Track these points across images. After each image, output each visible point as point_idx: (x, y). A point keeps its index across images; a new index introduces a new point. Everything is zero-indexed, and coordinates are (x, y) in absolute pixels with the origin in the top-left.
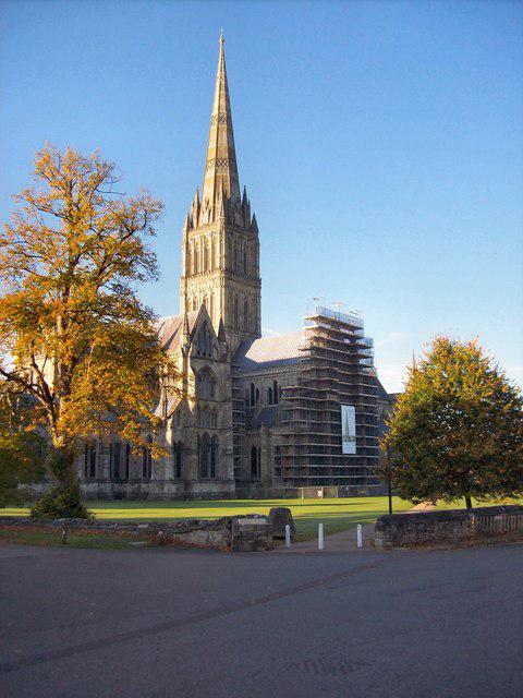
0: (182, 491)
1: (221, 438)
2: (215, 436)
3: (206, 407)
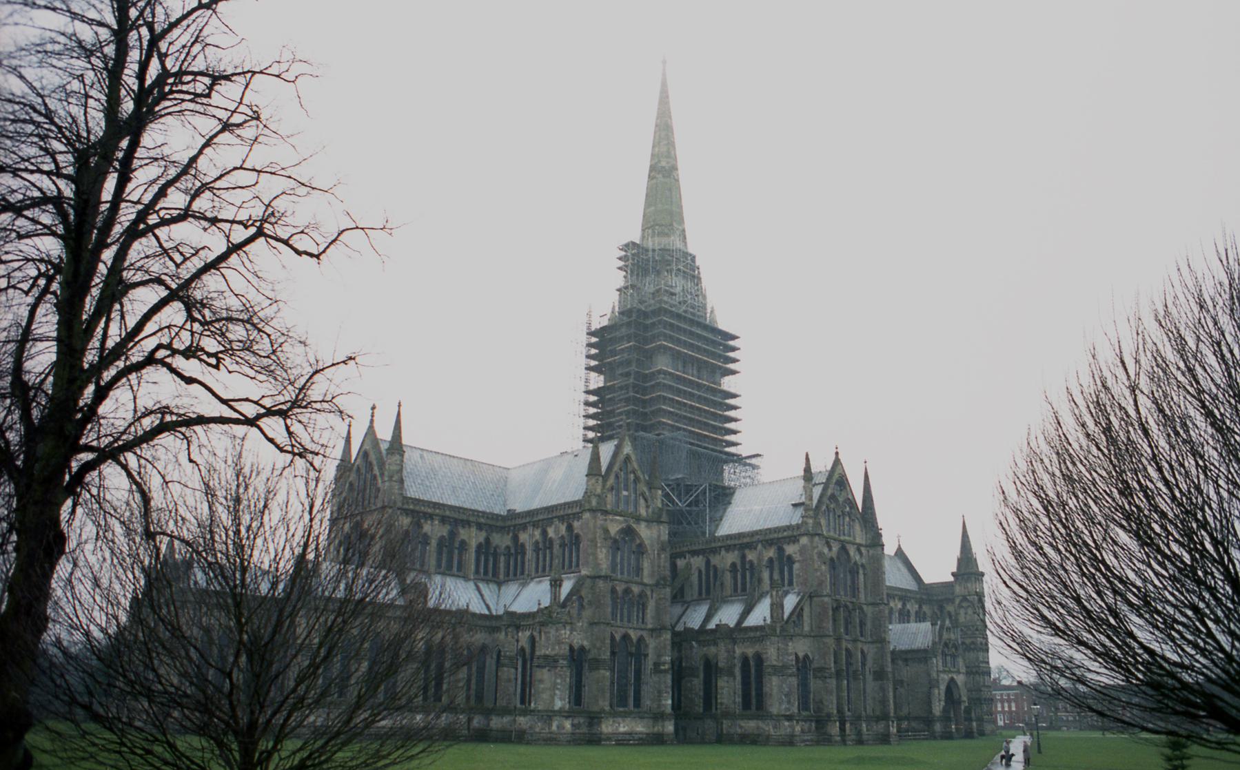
0: (584, 730)
1: (652, 644)
2: (641, 639)
3: (627, 591)
